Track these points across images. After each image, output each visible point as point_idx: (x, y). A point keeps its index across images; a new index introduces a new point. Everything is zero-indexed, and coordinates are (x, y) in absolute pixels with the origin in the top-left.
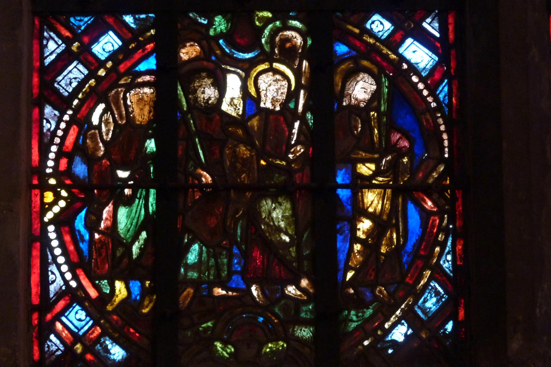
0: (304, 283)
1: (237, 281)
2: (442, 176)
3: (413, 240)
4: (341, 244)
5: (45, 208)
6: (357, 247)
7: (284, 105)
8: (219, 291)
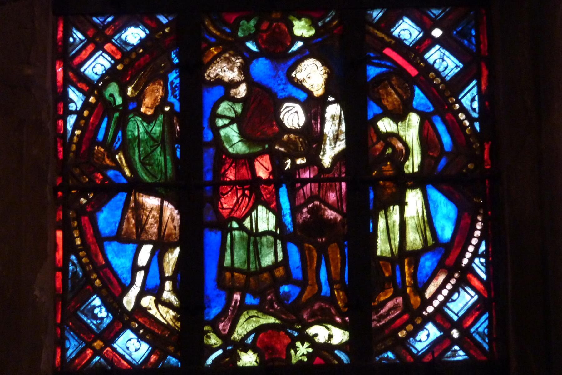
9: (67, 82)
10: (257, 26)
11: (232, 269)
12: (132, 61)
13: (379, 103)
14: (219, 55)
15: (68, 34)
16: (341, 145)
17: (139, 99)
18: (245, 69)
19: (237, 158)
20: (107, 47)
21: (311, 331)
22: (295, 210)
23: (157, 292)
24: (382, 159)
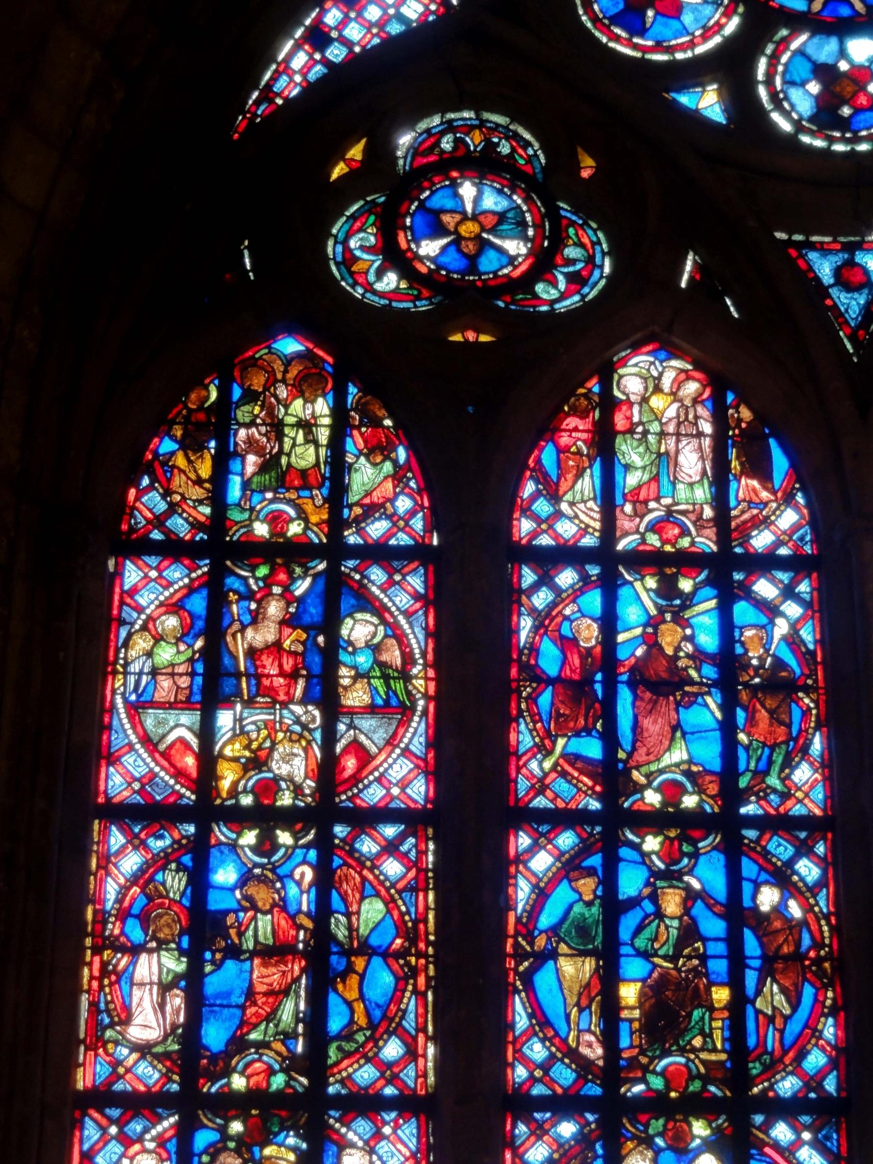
10: (665, 1126)
12: (566, 1152)
14: (634, 1149)
15: (514, 1126)
20: (545, 1138)
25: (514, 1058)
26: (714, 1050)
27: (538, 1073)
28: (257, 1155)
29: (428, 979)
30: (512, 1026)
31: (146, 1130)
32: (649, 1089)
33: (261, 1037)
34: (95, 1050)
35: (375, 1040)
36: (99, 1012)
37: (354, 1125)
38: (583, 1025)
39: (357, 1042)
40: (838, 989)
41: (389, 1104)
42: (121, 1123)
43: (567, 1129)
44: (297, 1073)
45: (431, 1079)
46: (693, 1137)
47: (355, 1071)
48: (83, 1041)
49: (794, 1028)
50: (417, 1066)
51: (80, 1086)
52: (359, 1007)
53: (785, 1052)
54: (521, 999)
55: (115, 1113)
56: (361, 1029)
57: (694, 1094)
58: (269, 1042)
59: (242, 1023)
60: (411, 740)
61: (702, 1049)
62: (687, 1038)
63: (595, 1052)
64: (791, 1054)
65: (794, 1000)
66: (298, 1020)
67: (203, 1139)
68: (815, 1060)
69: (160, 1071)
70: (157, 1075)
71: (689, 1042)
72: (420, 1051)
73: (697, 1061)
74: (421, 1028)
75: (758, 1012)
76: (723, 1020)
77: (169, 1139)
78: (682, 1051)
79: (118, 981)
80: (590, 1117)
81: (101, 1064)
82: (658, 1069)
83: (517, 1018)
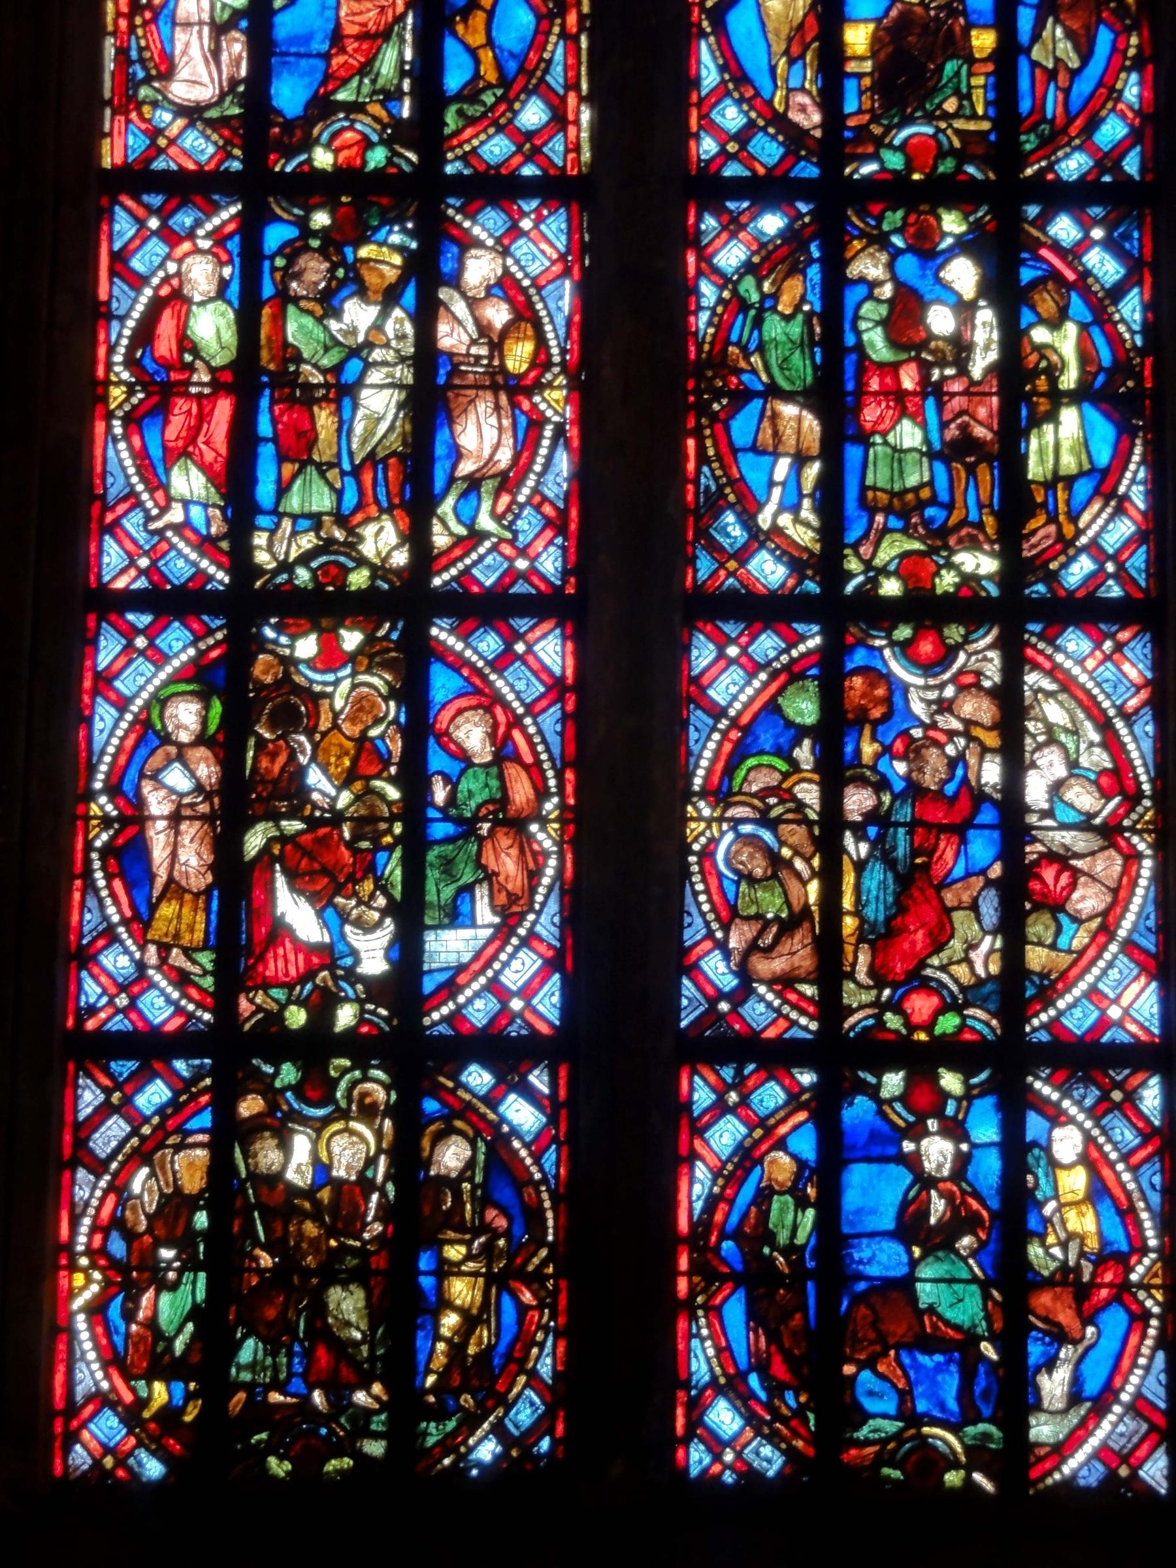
0: (377, 1388)
1: (298, 1385)
2: (544, 1263)
3: (506, 1338)
4: (422, 1341)
5: (71, 1294)
6: (441, 1346)
7: (361, 1174)
8: (276, 1397)
9: (700, 273)
10: (904, 219)
11: (874, 488)
12: (770, 253)
13: (1033, 308)
14: (863, 250)
15: (699, 219)
16: (993, 356)
17: (775, 296)
18: (891, 266)
19: (882, 367)
20: (742, 235)
21: (958, 558)
22: (943, 425)
23: (796, 509)
24: (1035, 373)
25: (700, 127)
26: (974, 116)
27: (732, 147)
28: (350, 258)
29: (581, 18)
30: (696, 82)
31: (198, 223)
32: (883, 169)
33: (352, 98)
34: (126, 114)
35: (509, 101)
36: (131, 63)
37: (481, 217)
38: (794, 83)
39: (484, 104)
40: (1146, 32)
41: (528, 188)
42: (165, 213)
43: (771, 223)
44: (402, 146)
45: (586, 155)
46: (944, 235)
47: (482, 143)
48: (110, 103)
49: (1084, 87)
50: (566, 136)
51: (107, 162)
52: (487, 56)
53: (1070, 120)
54: (709, 46)
55: (156, 200)
56: (490, 86)
57: (944, 176)
58: (365, 104)
59: (327, 77)
60: (116, 726)
61: (956, 115)
62: (937, 101)
63: (810, 118)
64: (1078, 122)
65: (1084, 50)
66: (403, 74)
67: (276, 236)
68: (1112, 131)
69: (215, 143)
70: (211, 150)
71: (939, 106)
72: (571, 117)
73: (949, 132)
74: (572, 85)
75: (1034, 64)
76: (987, 75)
77: (230, 236)
78: (929, 118)
79: (155, 19)
80: (803, 207)
81: (135, 135)
82: (896, 142)
83: (704, 73)
